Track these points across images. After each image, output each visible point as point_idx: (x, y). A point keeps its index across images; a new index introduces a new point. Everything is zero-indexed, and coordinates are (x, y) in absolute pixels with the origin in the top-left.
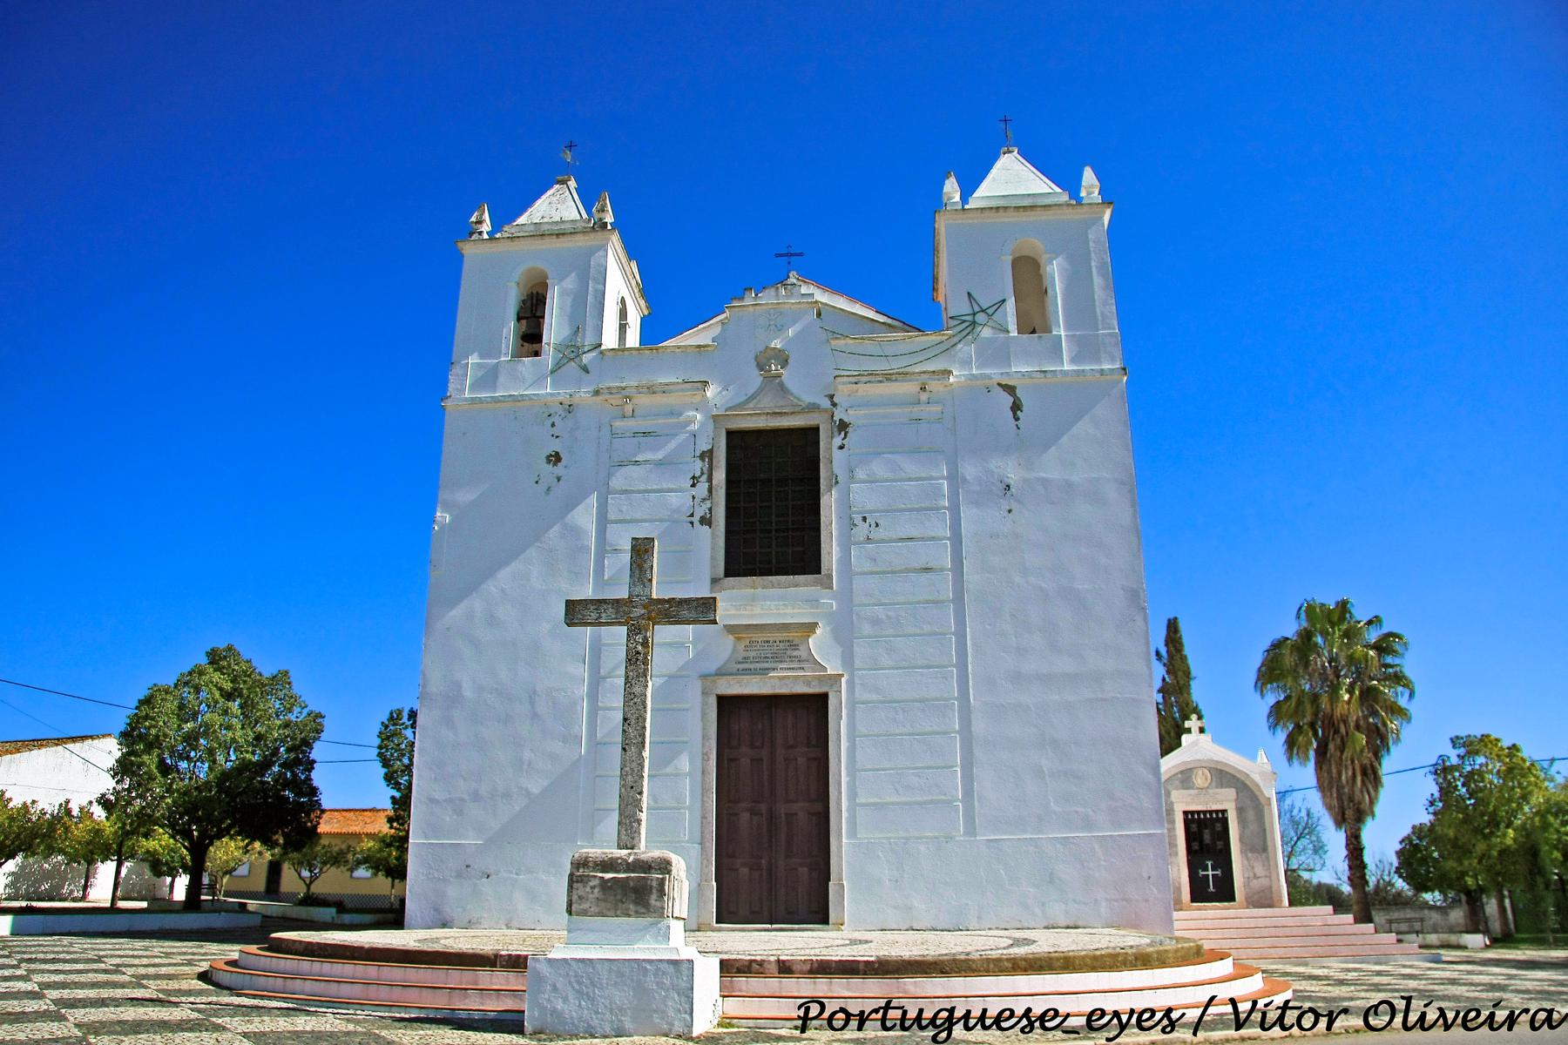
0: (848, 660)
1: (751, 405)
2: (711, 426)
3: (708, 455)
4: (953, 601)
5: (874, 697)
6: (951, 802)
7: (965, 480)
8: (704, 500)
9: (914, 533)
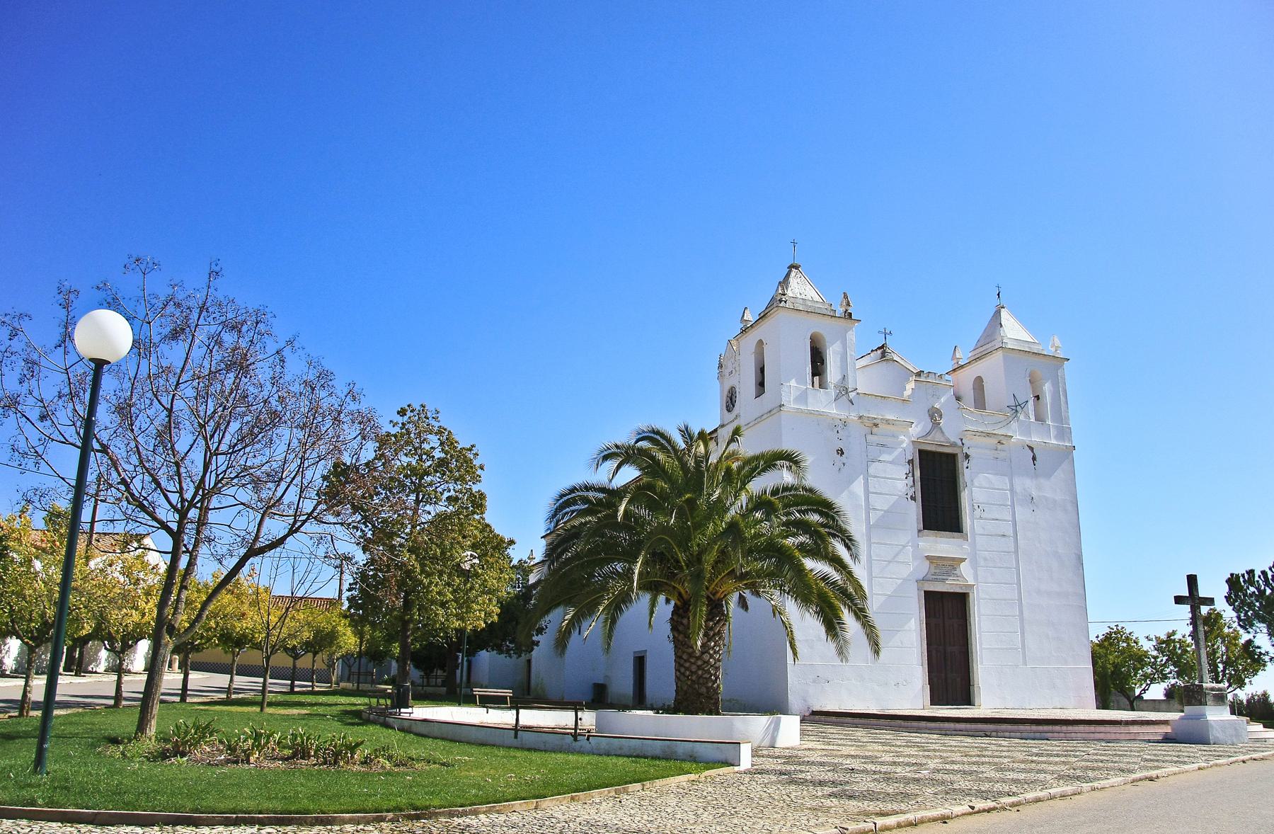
0: (976, 577)
1: (929, 438)
2: (912, 447)
3: (911, 462)
4: (1015, 552)
5: (987, 597)
6: (1016, 649)
7: (1016, 492)
8: (911, 487)
9: (997, 517)
